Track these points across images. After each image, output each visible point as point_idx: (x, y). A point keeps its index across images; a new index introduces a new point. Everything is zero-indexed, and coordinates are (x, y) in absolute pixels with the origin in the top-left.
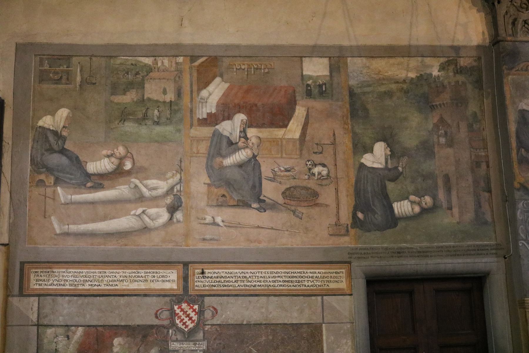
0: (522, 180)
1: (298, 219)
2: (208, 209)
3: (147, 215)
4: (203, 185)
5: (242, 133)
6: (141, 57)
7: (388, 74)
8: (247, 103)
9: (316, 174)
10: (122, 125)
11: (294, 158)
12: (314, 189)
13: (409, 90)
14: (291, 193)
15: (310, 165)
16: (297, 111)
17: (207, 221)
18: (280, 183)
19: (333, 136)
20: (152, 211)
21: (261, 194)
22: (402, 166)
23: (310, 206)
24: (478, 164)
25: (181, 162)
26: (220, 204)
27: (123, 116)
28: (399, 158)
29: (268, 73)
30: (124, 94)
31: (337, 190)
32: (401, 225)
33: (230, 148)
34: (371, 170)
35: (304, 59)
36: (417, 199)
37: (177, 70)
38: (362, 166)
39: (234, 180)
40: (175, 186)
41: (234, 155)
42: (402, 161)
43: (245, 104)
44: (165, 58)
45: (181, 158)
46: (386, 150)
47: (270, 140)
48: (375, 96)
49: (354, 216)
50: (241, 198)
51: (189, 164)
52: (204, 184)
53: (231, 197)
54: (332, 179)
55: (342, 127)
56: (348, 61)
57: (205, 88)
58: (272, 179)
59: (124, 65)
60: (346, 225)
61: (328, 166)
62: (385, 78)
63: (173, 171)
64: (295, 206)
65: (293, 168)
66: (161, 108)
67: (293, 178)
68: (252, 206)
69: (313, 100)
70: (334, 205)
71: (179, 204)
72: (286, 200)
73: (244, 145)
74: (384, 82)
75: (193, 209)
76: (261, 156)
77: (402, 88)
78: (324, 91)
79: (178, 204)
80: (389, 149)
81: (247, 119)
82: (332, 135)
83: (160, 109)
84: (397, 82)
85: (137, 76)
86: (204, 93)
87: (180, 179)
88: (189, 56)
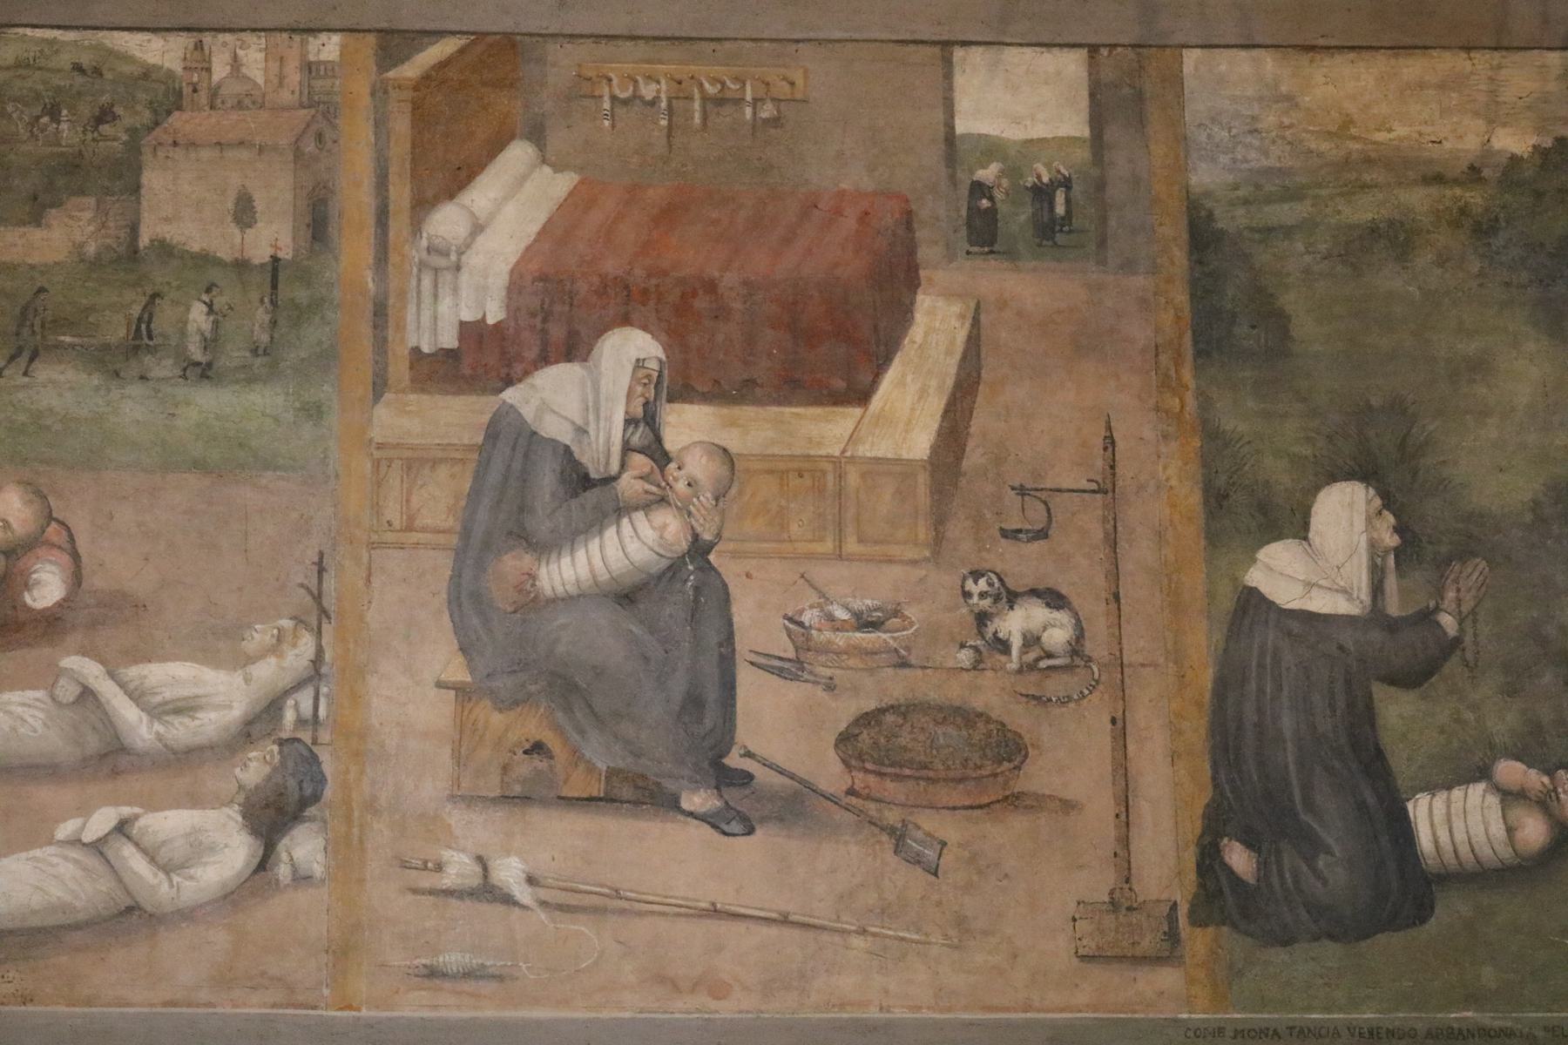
1: (919, 870)
2: (456, 817)
3: (137, 845)
4: (433, 692)
5: (637, 427)
6: (125, 34)
7: (1392, 136)
8: (665, 273)
9: (1016, 643)
10: (26, 379)
11: (901, 562)
12: (1006, 719)
13: (1497, 219)
14: (882, 740)
15: (982, 595)
16: (919, 317)
17: (449, 879)
18: (830, 687)
19: (1105, 449)
20: (168, 824)
21: (731, 743)
22: (1459, 605)
23: (980, 807)
25: (321, 571)
26: (517, 789)
27: (26, 331)
28: (1442, 564)
29: (775, 122)
30: (36, 219)
31: (1120, 727)
32: (1451, 909)
33: (574, 503)
34: (1295, 626)
35: (958, 53)
36: (1535, 780)
37: (310, 102)
38: (1252, 603)
39: (594, 667)
40: (287, 693)
41: (597, 540)
42: (1456, 581)
43: (654, 281)
44: (249, 37)
45: (321, 555)
46: (1377, 523)
47: (782, 466)
48: (1323, 247)
49: (1209, 860)
50: (630, 760)
51: (361, 584)
52: (440, 685)
53: (576, 755)
54: (1095, 669)
55: (1152, 402)
56: (1185, 70)
57: (451, 196)
58: (787, 665)
59: (38, 73)
60: (1166, 909)
61: (1076, 602)
62: (1373, 155)
63: (280, 617)
64: (903, 805)
65: (896, 613)
66: (221, 294)
67: (895, 660)
68: (685, 805)
69: (1006, 264)
70: (1101, 806)
71: (308, 791)
72: (859, 775)
73: (647, 492)
74: (1367, 177)
75: (376, 812)
76: (731, 546)
77: (1464, 211)
78: (1063, 218)
79: (301, 789)
80: (1391, 519)
81: (664, 358)
82: (1098, 442)
83: (220, 302)
84: (1439, 179)
85: (106, 129)
86: (447, 222)
87: (318, 660)
88: (369, 31)
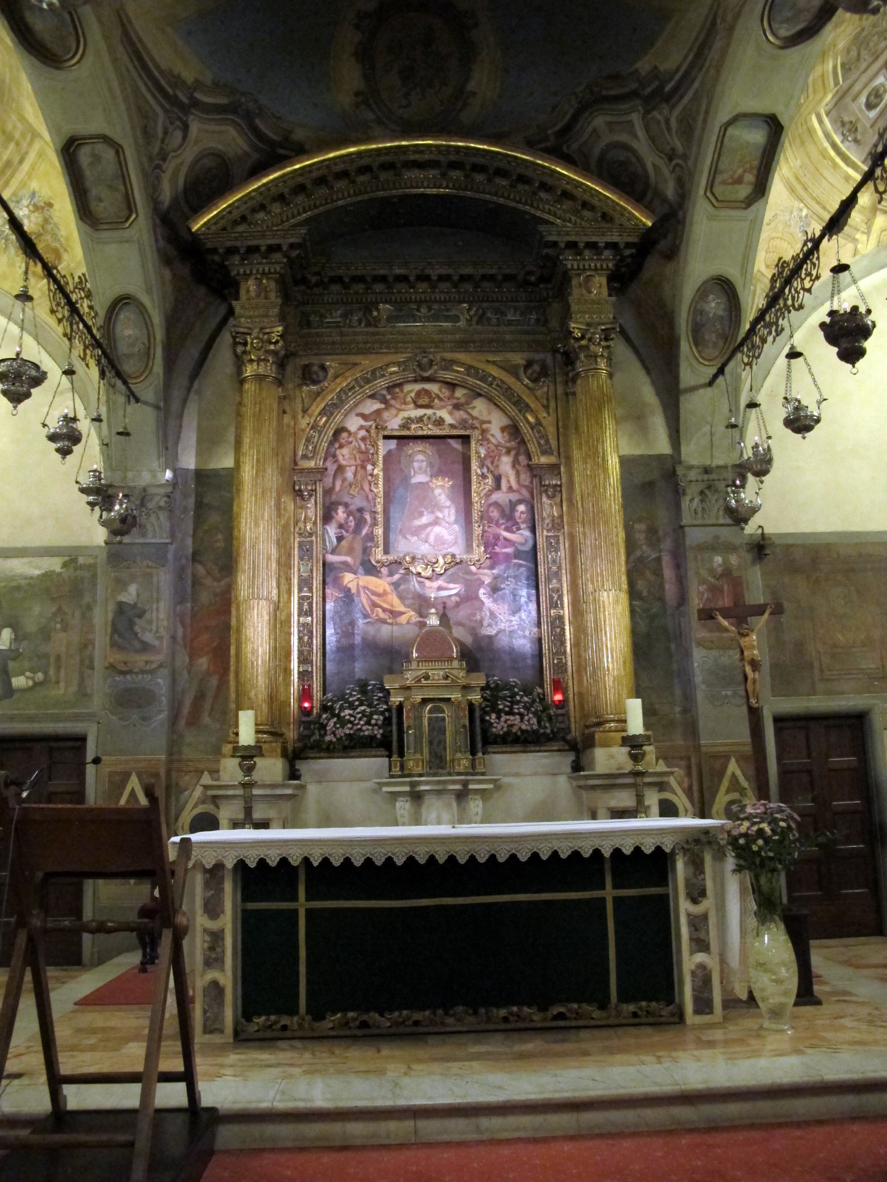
0: (112, 660)
24: (85, 646)
32: (16, 696)
36: (32, 675)
